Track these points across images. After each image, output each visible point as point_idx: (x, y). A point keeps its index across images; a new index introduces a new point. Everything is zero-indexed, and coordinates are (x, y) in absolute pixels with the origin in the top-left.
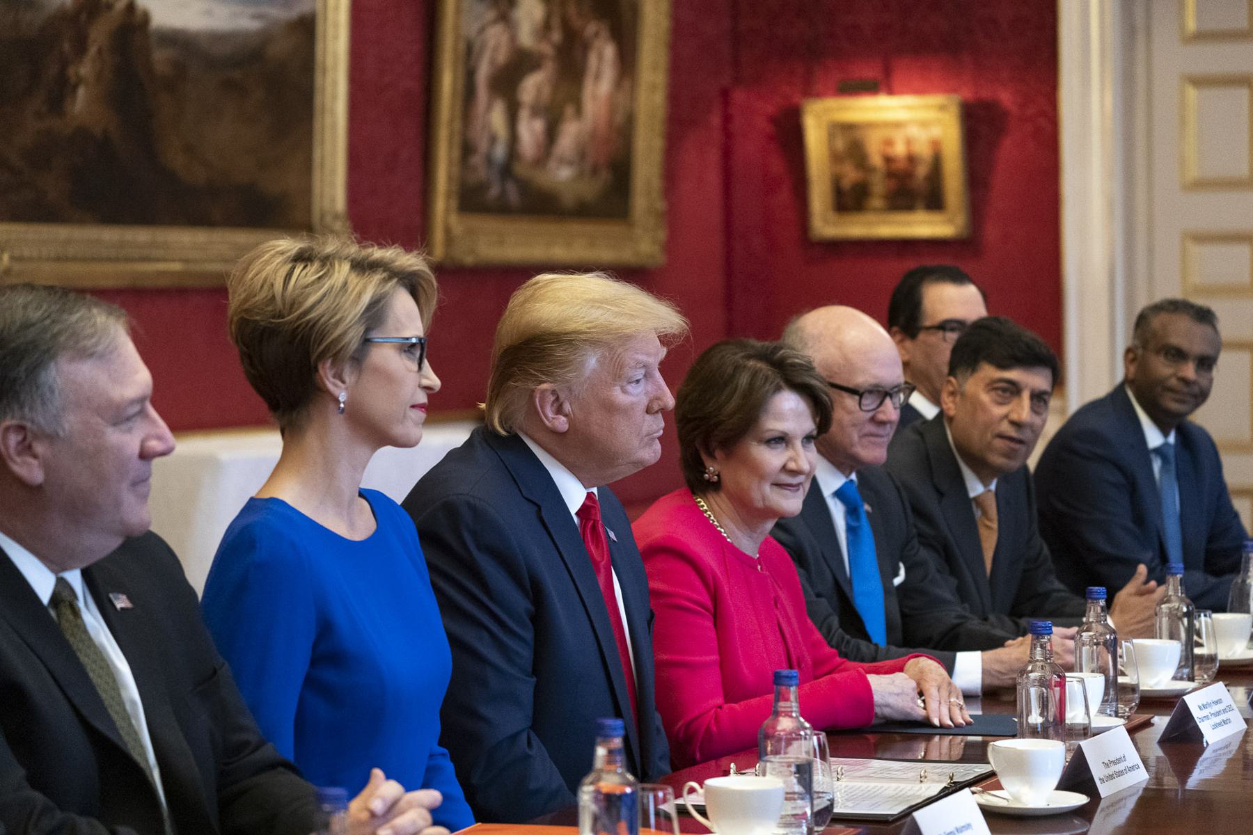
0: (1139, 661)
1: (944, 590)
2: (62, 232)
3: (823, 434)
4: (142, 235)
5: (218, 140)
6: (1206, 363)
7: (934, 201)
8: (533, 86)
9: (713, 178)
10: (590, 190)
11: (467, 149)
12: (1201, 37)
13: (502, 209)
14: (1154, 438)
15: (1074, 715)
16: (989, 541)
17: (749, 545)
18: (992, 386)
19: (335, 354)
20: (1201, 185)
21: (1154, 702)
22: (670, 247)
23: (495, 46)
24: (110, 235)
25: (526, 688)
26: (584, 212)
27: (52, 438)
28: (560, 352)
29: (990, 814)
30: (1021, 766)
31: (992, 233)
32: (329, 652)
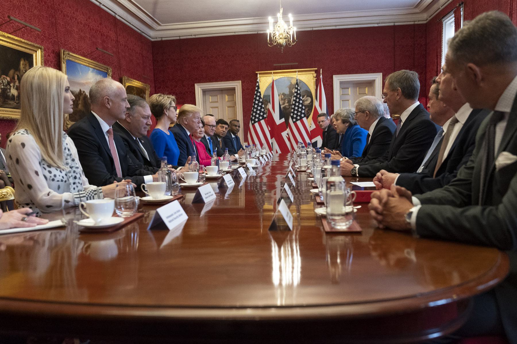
14: (233, 136)
19: (166, 108)
27: (133, 116)
28: (187, 113)
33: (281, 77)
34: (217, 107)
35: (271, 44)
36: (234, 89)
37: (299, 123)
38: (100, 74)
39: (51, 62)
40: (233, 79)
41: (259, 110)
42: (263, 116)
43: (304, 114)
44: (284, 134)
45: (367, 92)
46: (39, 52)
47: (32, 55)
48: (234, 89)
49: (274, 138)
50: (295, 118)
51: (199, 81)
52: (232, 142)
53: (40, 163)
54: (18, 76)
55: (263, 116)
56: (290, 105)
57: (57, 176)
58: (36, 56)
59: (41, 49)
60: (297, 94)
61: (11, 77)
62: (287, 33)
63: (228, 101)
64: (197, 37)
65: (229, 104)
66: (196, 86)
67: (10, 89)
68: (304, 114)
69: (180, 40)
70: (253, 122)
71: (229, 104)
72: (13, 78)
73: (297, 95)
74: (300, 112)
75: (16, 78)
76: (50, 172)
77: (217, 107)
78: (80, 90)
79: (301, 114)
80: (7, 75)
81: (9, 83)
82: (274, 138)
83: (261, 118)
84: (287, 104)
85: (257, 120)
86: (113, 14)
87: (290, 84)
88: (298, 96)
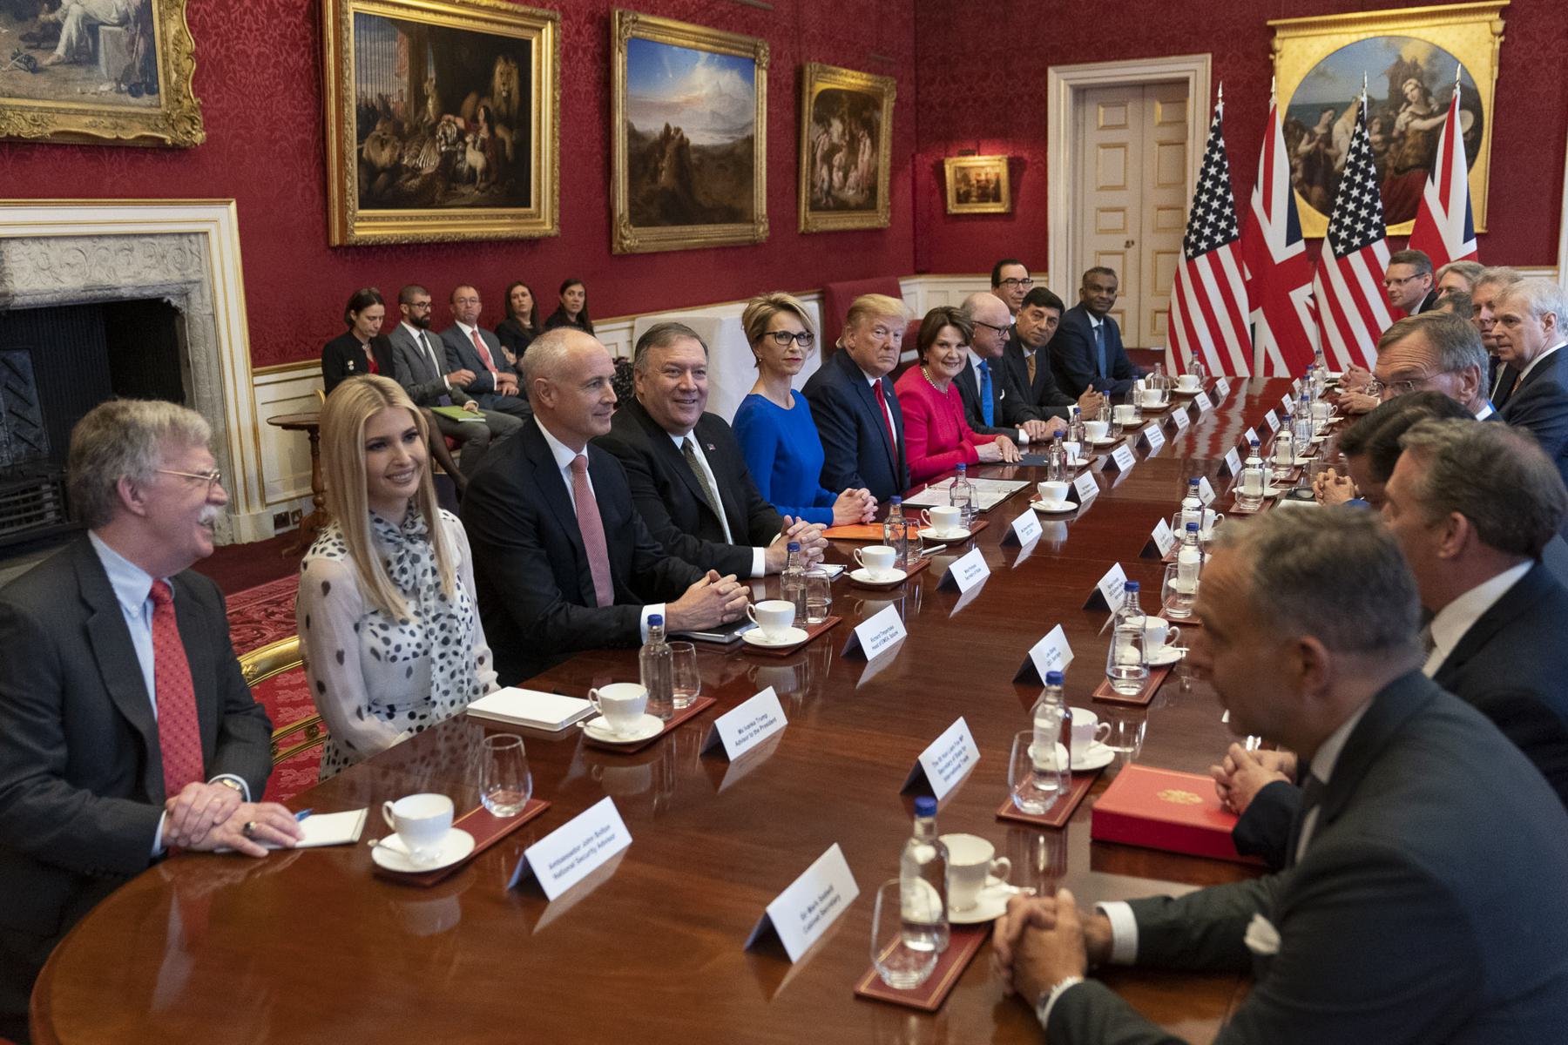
0: (1094, 431)
1: (1017, 397)
2: (658, 229)
3: (968, 340)
4: (688, 229)
5: (715, 188)
6: (1111, 290)
7: (997, 199)
8: (838, 158)
9: (909, 190)
10: (860, 199)
11: (813, 185)
12: (1104, 127)
13: (827, 209)
14: (1095, 323)
15: (1070, 462)
16: (1032, 375)
17: (943, 390)
18: (1033, 313)
20: (1103, 188)
21: (1100, 448)
22: (892, 220)
23: (823, 144)
24: (677, 229)
25: (854, 455)
26: (858, 208)
30: (1051, 493)
31: (1019, 210)
32: (781, 455)
33: (1363, 36)
34: (1123, 145)
36: (1184, 82)
37: (1356, 259)
38: (732, 67)
39: (585, 51)
41: (1215, 212)
42: (1226, 232)
44: (1300, 297)
46: (548, 32)
47: (529, 43)
48: (1184, 82)
49: (1260, 310)
50: (1343, 242)
52: (1087, 344)
54: (487, 109)
55: (1226, 232)
56: (1388, 141)
57: (404, 647)
58: (540, 43)
59: (553, 21)
60: (1359, 156)
61: (468, 116)
63: (1162, 124)
65: (1168, 134)
67: (464, 152)
70: (1190, 252)
71: (1168, 134)
72: (475, 119)
73: (1357, 159)
74: (1363, 220)
75: (481, 117)
77: (1123, 145)
78: (667, 127)
79: (1367, 228)
80: (457, 114)
81: (461, 135)
82: (1260, 310)
83: (1219, 238)
85: (1203, 245)
87: (1395, 60)
88: (1362, 164)
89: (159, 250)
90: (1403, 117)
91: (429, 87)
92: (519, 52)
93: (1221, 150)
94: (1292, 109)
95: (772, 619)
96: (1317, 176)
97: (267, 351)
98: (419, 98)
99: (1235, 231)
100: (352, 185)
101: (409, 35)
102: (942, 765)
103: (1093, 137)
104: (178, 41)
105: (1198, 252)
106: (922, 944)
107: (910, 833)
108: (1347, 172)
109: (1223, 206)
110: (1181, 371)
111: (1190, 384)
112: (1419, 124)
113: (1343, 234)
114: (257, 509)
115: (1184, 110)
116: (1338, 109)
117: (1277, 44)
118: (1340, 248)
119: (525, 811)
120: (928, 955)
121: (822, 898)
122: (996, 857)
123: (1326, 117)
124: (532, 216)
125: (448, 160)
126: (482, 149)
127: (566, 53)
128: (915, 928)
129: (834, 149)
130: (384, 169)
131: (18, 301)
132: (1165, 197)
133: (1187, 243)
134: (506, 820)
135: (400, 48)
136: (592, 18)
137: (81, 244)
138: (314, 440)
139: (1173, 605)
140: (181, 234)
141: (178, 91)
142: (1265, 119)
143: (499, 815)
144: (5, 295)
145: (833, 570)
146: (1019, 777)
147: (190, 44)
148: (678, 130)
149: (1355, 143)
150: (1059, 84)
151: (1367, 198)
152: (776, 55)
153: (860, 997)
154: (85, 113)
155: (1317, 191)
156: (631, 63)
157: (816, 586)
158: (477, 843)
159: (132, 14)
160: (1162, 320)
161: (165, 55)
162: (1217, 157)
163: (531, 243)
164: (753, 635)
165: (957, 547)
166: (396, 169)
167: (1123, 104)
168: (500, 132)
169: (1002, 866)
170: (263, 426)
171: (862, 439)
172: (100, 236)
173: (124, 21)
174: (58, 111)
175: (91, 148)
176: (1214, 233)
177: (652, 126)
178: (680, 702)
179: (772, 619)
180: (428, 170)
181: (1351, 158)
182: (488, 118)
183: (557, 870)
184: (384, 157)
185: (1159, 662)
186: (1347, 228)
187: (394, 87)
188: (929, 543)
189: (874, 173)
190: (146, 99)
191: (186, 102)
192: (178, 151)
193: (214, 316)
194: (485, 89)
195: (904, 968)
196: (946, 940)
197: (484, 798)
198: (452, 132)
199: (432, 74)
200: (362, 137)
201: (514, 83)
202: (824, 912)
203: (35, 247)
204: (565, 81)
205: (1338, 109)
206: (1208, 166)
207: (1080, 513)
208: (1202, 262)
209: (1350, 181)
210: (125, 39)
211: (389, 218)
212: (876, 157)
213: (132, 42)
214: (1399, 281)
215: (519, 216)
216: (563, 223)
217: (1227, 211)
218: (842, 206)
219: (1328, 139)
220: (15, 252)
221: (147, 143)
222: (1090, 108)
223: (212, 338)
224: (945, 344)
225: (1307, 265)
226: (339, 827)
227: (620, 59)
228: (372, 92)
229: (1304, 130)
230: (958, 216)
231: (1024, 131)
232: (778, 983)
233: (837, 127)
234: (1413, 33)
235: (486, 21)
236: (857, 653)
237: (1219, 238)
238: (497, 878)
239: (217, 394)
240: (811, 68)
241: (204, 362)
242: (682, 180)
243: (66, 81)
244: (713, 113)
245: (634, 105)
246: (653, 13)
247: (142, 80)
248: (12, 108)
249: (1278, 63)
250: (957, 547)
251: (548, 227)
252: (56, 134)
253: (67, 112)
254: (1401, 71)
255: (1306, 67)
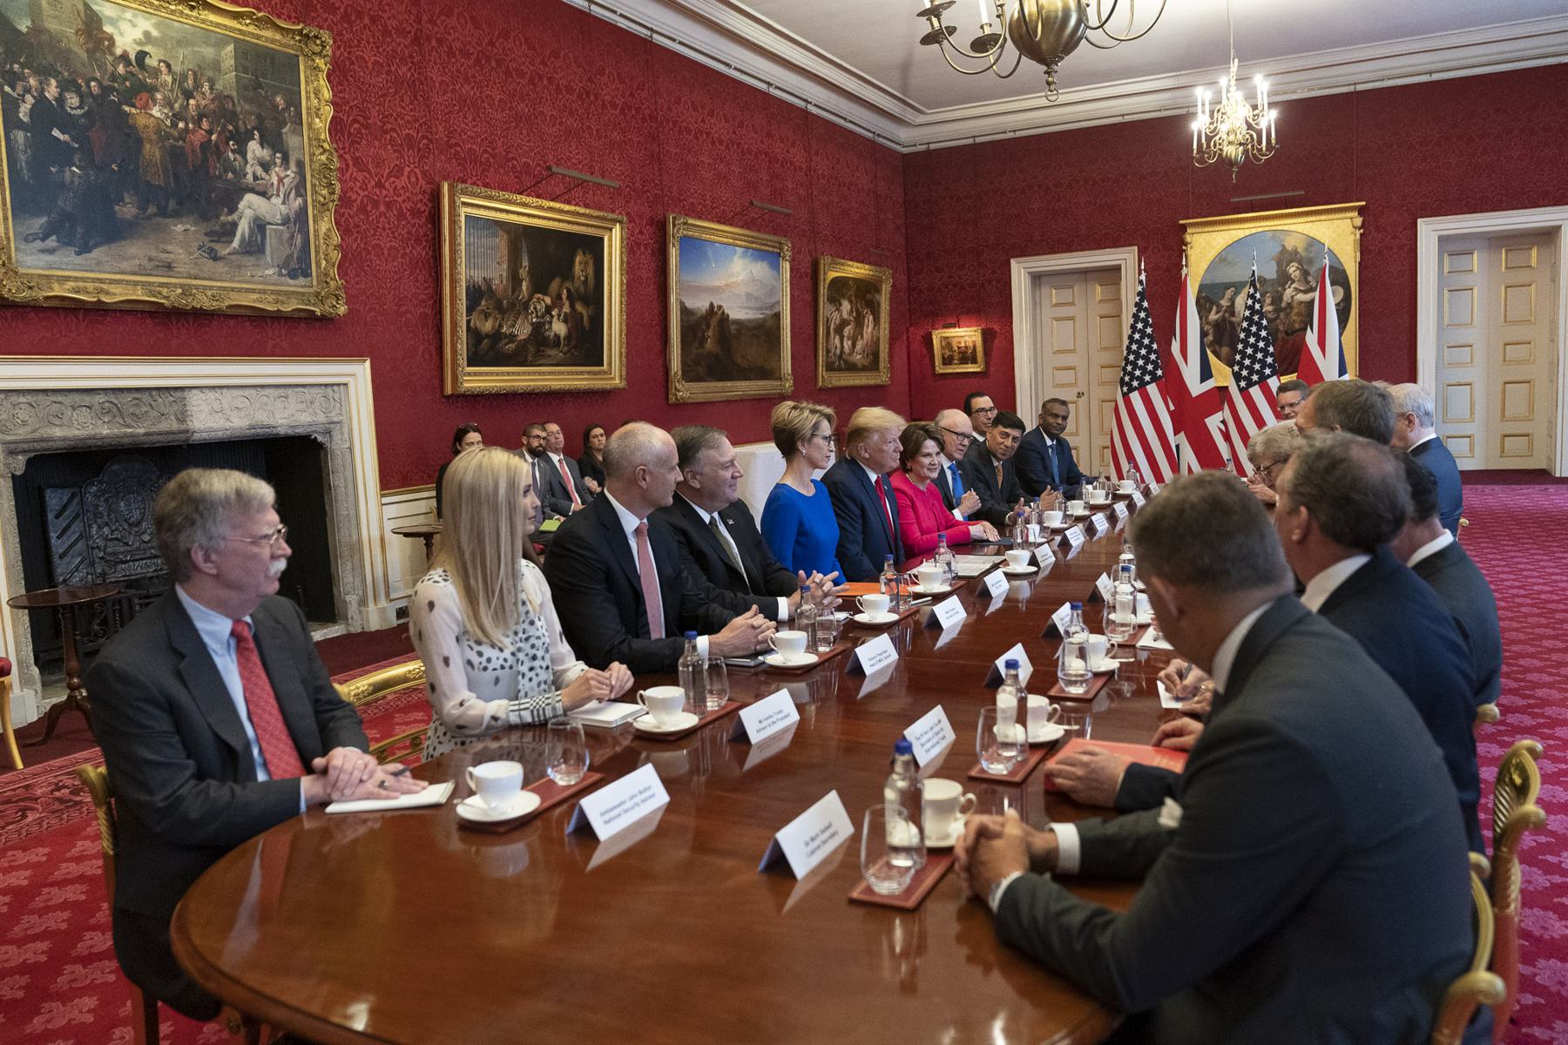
0: (1049, 518)
2: (705, 384)
4: (729, 384)
5: (750, 353)
6: (1065, 418)
7: (974, 361)
8: (847, 330)
10: (866, 362)
11: (828, 351)
13: (840, 369)
14: (1049, 442)
15: (1031, 539)
16: (1000, 480)
21: (1055, 531)
22: (891, 378)
23: (836, 318)
25: (860, 538)
26: (865, 369)
29: (1007, 575)
30: (1016, 559)
34: (1072, 318)
35: (1202, 161)
36: (1118, 268)
37: (1255, 391)
39: (646, 246)
40: (1116, 244)
41: (1143, 357)
42: (1152, 373)
43: (1270, 366)
44: (1213, 423)
45: (1534, 262)
48: (1118, 268)
50: (1245, 378)
51: (1023, 253)
52: (1043, 458)
53: (457, 639)
54: (569, 291)
55: (1152, 373)
56: (1278, 310)
58: (610, 240)
62: (1250, 127)
64: (1019, 134)
65: (1107, 309)
66: (1015, 264)
68: (1270, 366)
69: (974, 145)
71: (1107, 309)
72: (559, 297)
74: (1260, 361)
76: (480, 654)
77: (1072, 318)
78: (712, 305)
79: (1263, 368)
80: (545, 294)
81: (548, 310)
83: (1147, 378)
84: (1270, 308)
85: (1135, 384)
86: (801, 104)
88: (1256, 318)
89: (308, 397)
90: (1289, 292)
91: (523, 273)
92: (594, 246)
93: (1146, 310)
94: (1202, 288)
95: (789, 644)
96: (1222, 337)
97: (393, 477)
98: (515, 280)
99: (1159, 372)
100: (462, 348)
101: (508, 233)
102: (923, 740)
103: (1048, 313)
104: (327, 236)
105: (1131, 389)
106: (901, 862)
107: (892, 770)
108: (1245, 324)
109: (1149, 353)
110: (1121, 477)
111: (1128, 487)
112: (1301, 297)
113: (1245, 373)
114: (383, 603)
115: (1119, 290)
116: (1238, 287)
117: (1188, 238)
118: (1243, 384)
119: (584, 779)
120: (908, 869)
121: (823, 832)
122: (964, 794)
123: (1229, 293)
124: (605, 373)
125: (538, 329)
126: (565, 321)
127: (631, 247)
128: (897, 850)
129: (844, 323)
130: (487, 336)
131: (197, 436)
132: (1107, 358)
133: (1122, 383)
134: (569, 787)
135: (501, 242)
136: (651, 222)
137: (247, 392)
138: (428, 545)
139: (1113, 631)
140: (326, 385)
141: (326, 275)
142: (1179, 288)
143: (561, 783)
144: (187, 431)
145: (842, 616)
146: (985, 748)
147: (336, 239)
148: (720, 307)
149: (1250, 302)
150: (1020, 272)
151: (1261, 344)
152: (796, 251)
153: (853, 902)
154: (253, 291)
155: (1225, 350)
156: (682, 254)
157: (826, 626)
158: (543, 800)
159: (292, 216)
160: (1108, 453)
161: (317, 247)
162: (1142, 315)
163: (604, 394)
164: (773, 659)
165: (939, 598)
166: (496, 336)
167: (1071, 287)
168: (579, 307)
169: (970, 801)
170: (389, 536)
171: (866, 530)
172: (262, 386)
173: (286, 221)
174: (233, 289)
175: (258, 318)
176: (1143, 374)
177: (700, 304)
178: (712, 704)
179: (789, 644)
180: (522, 337)
181: (1247, 313)
182: (569, 297)
183: (607, 817)
184: (488, 326)
185: (1103, 669)
186: (1247, 368)
187: (496, 272)
188: (917, 596)
189: (877, 343)
190: (302, 281)
191: (332, 283)
192: (325, 320)
193: (351, 449)
194: (567, 275)
195: (889, 878)
196: (924, 861)
197: (549, 771)
198: (541, 307)
199: (525, 263)
200: (470, 311)
201: (590, 270)
202: (824, 842)
203: (211, 395)
204: (630, 269)
205: (1238, 287)
206: (1136, 322)
207: (1042, 575)
208: (1135, 397)
209: (1247, 331)
210: (286, 235)
211: (492, 374)
212: (876, 330)
213: (292, 237)
214: (1291, 405)
215: (595, 373)
216: (629, 378)
217: (1153, 357)
218: (851, 367)
219: (1231, 310)
220: (196, 402)
221: (302, 315)
222: (1045, 290)
223: (349, 467)
224: (929, 455)
225: (1219, 397)
226: (435, 793)
227: (673, 253)
228: (478, 276)
229: (1212, 303)
230: (943, 375)
231: (994, 308)
232: (788, 894)
233: (846, 306)
234: (1293, 228)
235: (569, 222)
236: (858, 672)
237: (1147, 378)
238: (559, 828)
239: (352, 512)
240: (825, 261)
241: (342, 485)
242: (724, 346)
243: (239, 267)
244: (748, 295)
245: (685, 288)
246: (700, 218)
247: (299, 266)
248: (197, 288)
249: (1190, 252)
250: (939, 598)
251: (617, 381)
252: (230, 307)
253: (240, 290)
254: (1285, 257)
255: (1211, 255)
